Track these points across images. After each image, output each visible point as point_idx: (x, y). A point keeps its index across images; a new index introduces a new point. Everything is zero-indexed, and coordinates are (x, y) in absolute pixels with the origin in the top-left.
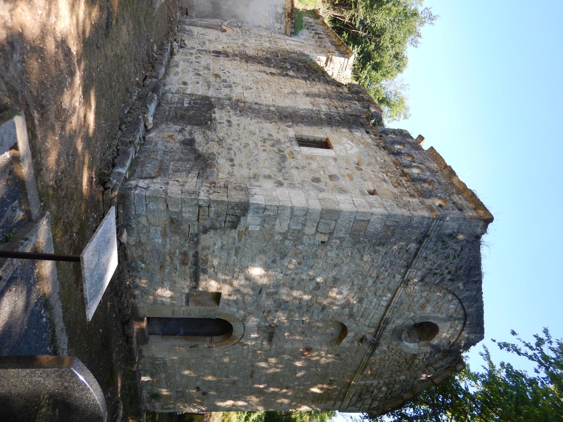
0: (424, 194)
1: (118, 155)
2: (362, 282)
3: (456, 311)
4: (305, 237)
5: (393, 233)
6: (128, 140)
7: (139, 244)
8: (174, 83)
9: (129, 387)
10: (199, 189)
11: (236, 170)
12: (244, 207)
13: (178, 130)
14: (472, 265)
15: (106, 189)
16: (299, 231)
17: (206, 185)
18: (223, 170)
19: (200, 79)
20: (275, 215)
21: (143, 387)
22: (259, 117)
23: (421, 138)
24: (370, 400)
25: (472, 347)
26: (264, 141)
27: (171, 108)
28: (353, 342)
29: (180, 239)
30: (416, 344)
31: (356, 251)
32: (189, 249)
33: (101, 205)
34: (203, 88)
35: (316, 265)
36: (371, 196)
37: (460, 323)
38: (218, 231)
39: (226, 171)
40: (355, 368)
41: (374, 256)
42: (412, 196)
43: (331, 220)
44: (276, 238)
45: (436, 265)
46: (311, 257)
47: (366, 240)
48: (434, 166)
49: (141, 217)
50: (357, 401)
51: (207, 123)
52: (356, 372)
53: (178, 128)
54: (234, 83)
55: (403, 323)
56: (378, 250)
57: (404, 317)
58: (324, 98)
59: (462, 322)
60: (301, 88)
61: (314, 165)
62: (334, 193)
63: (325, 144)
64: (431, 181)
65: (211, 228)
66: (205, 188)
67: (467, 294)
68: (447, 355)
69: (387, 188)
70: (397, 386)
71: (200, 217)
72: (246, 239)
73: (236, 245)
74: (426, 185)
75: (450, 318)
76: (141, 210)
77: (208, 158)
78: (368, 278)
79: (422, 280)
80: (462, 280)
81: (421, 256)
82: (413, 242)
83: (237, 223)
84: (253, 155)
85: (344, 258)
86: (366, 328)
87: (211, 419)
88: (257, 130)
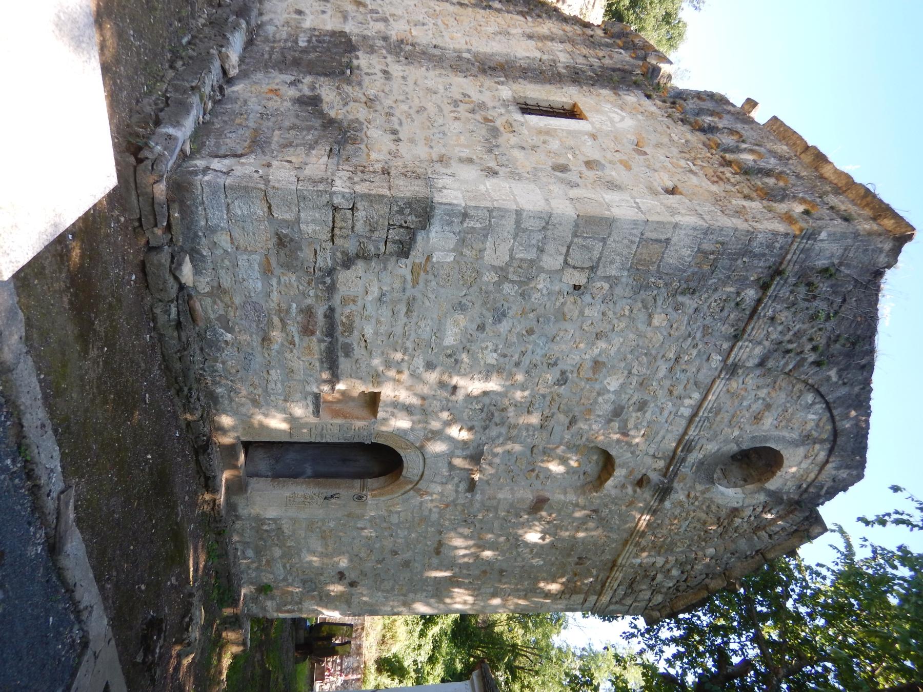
0: (769, 195)
2: (648, 368)
3: (817, 425)
4: (543, 276)
5: (714, 267)
6: (187, 85)
7: (218, 291)
8: (279, 11)
9: (217, 573)
11: (403, 148)
12: (424, 209)
14: (859, 332)
15: (140, 161)
16: (532, 263)
17: (346, 167)
18: (378, 146)
19: (329, 7)
20: (483, 229)
21: (242, 572)
22: (443, 67)
23: (751, 103)
24: (649, 593)
25: (841, 494)
26: (456, 103)
27: (273, 48)
28: (623, 486)
29: (299, 278)
30: (739, 490)
31: (640, 305)
32: (317, 301)
33: (134, 197)
34: (333, 19)
35: (562, 334)
36: (671, 196)
37: (823, 450)
38: (373, 264)
39: (385, 150)
40: (625, 535)
41: (674, 315)
42: (747, 197)
43: (594, 239)
44: (485, 279)
45: (791, 333)
46: (553, 318)
47: (661, 283)
48: (782, 148)
49: (219, 234)
50: (626, 595)
51: (343, 73)
52: (626, 542)
55: (718, 450)
56: (682, 304)
57: (721, 438)
58: (560, 42)
59: (828, 446)
60: (516, 28)
61: (555, 145)
62: (598, 189)
63: (572, 113)
65: (358, 256)
66: (345, 173)
67: (843, 391)
68: (795, 509)
69: (699, 183)
70: (698, 567)
71: (337, 231)
72: (427, 282)
73: (408, 293)
74: (771, 181)
75: (807, 439)
76: (218, 217)
78: (660, 362)
79: (761, 364)
80: (837, 364)
81: (765, 316)
82: (750, 286)
83: (410, 244)
84: (435, 124)
85: (615, 322)
86: (649, 460)
87: (364, 634)
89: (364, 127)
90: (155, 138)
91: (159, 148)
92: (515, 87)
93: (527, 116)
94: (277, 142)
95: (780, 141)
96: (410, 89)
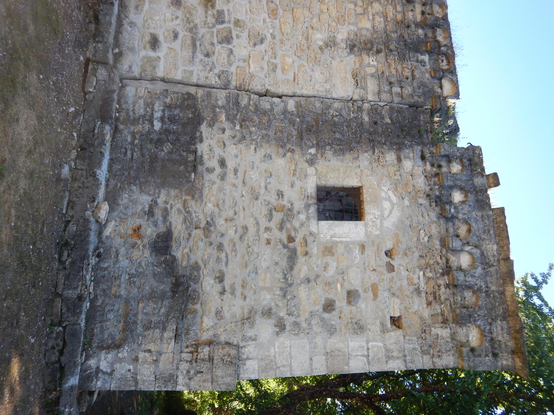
10: (178, 369)
13: (147, 209)
22: (268, 142)
23: (495, 180)
27: (133, 134)
39: (213, 310)
42: (445, 321)
48: (491, 248)
51: (188, 181)
53: (145, 199)
54: (237, 23)
58: (378, 52)
64: (478, 289)
74: (468, 294)
77: (190, 278)
88: (263, 185)
90: (63, 400)
91: (67, 410)
92: (321, 165)
94: (141, 322)
95: (496, 236)
96: (237, 195)
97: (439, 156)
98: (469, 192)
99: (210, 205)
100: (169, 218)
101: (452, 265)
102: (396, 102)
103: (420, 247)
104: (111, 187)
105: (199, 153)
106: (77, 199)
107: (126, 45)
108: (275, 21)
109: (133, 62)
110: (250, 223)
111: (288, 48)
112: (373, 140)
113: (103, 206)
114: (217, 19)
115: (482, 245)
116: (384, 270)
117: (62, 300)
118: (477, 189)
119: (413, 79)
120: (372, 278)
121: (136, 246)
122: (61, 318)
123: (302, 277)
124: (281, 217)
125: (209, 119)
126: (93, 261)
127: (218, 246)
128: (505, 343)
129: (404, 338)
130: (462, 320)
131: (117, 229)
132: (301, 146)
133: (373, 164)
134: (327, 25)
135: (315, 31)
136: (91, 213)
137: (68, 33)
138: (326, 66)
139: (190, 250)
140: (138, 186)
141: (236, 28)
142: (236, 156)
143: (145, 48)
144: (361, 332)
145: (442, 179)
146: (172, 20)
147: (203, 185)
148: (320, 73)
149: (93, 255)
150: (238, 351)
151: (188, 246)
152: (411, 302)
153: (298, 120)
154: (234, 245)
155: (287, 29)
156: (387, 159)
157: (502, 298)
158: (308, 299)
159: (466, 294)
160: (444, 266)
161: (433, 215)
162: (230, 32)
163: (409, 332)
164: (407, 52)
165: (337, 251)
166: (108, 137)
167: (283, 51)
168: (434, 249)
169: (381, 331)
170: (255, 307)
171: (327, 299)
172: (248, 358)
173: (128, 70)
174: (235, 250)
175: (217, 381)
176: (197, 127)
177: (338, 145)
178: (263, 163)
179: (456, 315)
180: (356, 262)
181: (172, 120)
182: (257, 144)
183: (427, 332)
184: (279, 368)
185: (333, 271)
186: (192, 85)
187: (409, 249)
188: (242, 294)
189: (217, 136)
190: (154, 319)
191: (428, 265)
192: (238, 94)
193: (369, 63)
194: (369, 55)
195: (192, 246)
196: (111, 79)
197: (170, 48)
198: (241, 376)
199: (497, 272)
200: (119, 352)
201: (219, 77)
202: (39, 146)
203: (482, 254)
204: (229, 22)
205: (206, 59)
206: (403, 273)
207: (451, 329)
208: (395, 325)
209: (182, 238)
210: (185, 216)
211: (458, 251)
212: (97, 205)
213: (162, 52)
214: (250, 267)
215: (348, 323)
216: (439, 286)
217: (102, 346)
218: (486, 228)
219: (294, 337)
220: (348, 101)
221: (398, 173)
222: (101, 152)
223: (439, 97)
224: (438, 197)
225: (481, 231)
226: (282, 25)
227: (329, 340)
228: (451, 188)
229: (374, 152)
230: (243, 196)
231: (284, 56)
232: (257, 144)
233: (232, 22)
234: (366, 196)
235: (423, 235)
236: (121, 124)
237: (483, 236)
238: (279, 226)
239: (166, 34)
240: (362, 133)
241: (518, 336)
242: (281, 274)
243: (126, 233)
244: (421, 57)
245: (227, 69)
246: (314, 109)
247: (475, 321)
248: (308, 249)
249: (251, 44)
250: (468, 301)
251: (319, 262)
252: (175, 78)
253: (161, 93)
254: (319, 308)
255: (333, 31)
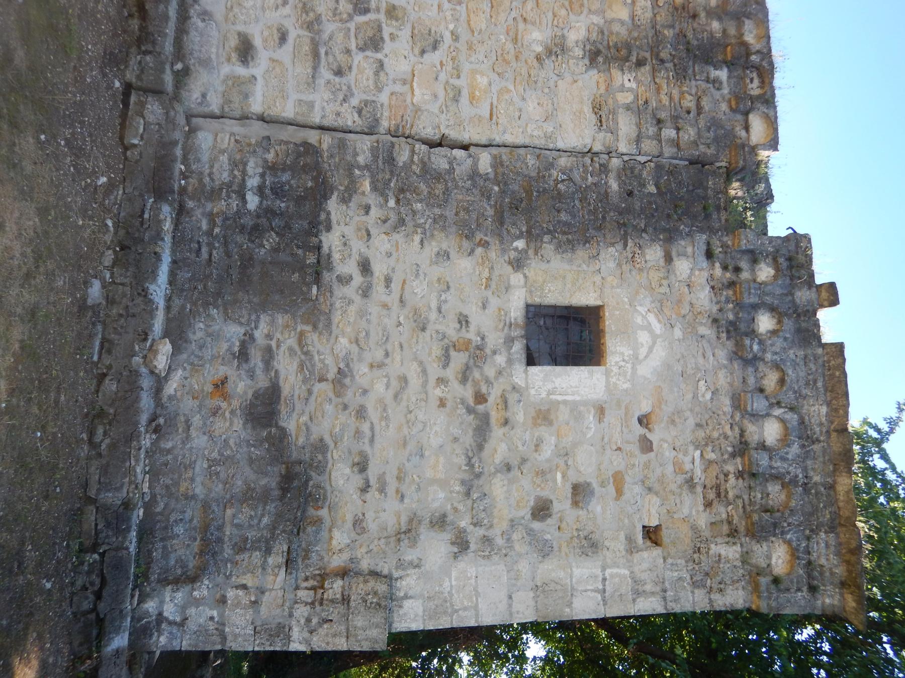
1: (103, 582)
10: (291, 615)
13: (236, 349)
22: (444, 228)
23: (830, 295)
27: (211, 217)
34: (299, 69)
39: (349, 518)
42: (733, 533)
48: (817, 411)
51: (307, 300)
53: (234, 332)
54: (392, 12)
58: (640, 63)
64: (790, 481)
74: (774, 489)
77: (311, 465)
84: (415, 431)
88: (434, 305)
89: (329, 455)
92: (535, 269)
93: (533, 369)
94: (230, 539)
95: (826, 390)
96: (389, 322)
97: (736, 251)
98: (786, 315)
99: (343, 341)
100: (275, 363)
101: (749, 440)
102: (666, 155)
103: (697, 409)
104: (175, 311)
105: (325, 249)
106: (117, 337)
107: (195, 55)
108: (458, 8)
109: (207, 87)
110: (412, 371)
111: (481, 57)
112: (624, 225)
113: (161, 347)
114: (356, 5)
115: (802, 406)
116: (635, 448)
117: (97, 508)
118: (800, 311)
119: (699, 114)
120: (615, 464)
121: (220, 412)
122: (96, 539)
123: (497, 461)
124: (464, 361)
125: (342, 188)
126: (146, 441)
127: (358, 412)
128: (831, 569)
129: (665, 561)
130: (762, 531)
131: (186, 383)
132: (500, 236)
133: (624, 267)
134: (550, 15)
135: (529, 27)
136: (141, 360)
137: (90, 47)
138: (546, 90)
139: (311, 418)
140: (221, 308)
141: (389, 22)
142: (389, 255)
143: (229, 60)
144: (593, 553)
145: (741, 293)
146: (277, 8)
147: (331, 305)
148: (536, 104)
149: (147, 432)
150: (391, 586)
151: (307, 411)
152: (678, 501)
153: (496, 188)
154: (385, 410)
155: (480, 22)
156: (648, 258)
157: (829, 495)
158: (508, 498)
159: (770, 489)
160: (736, 442)
161: (722, 355)
162: (380, 29)
163: (673, 551)
164: (691, 63)
165: (557, 417)
166: (168, 226)
167: (471, 63)
168: (721, 413)
169: (627, 551)
170: (419, 513)
171: (538, 499)
172: (406, 597)
173: (199, 100)
174: (387, 418)
175: (356, 636)
176: (321, 204)
177: (564, 233)
178: (435, 267)
179: (753, 524)
180: (589, 436)
181: (278, 191)
182: (425, 234)
183: (703, 550)
184: (457, 611)
185: (549, 452)
186: (312, 128)
187: (679, 412)
188: (397, 491)
189: (357, 219)
190: (251, 534)
191: (709, 440)
192: (392, 143)
193: (623, 85)
194: (622, 70)
195: (313, 410)
196: (170, 120)
197: (272, 60)
198: (394, 625)
199: (824, 452)
200: (193, 589)
201: (360, 112)
202: (44, 262)
203: (802, 422)
204: (378, 10)
205: (337, 79)
206: (667, 454)
207: (742, 545)
208: (650, 538)
209: (296, 397)
210: (301, 361)
211: (762, 416)
212: (151, 346)
213: (259, 68)
214: (411, 446)
215: (572, 538)
216: (726, 475)
217: (166, 579)
218: (810, 377)
219: (483, 562)
220: (584, 154)
221: (665, 282)
222: (155, 253)
223: (743, 146)
224: (732, 323)
225: (802, 383)
226: (472, 15)
227: (541, 566)
228: (755, 307)
229: (625, 245)
230: (400, 324)
231: (474, 72)
232: (424, 233)
233: (383, 11)
234: (610, 323)
235: (704, 389)
236: (191, 198)
237: (804, 392)
238: (460, 376)
239: (266, 33)
240: (607, 212)
241: (853, 559)
242: (463, 457)
243: (203, 391)
244: (714, 73)
245: (374, 98)
246: (524, 169)
247: (783, 533)
248: (508, 414)
249: (417, 51)
250: (773, 500)
251: (527, 436)
252: (284, 115)
253: (259, 144)
254: (526, 512)
255: (561, 25)
